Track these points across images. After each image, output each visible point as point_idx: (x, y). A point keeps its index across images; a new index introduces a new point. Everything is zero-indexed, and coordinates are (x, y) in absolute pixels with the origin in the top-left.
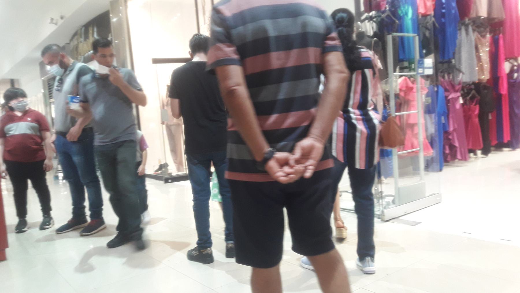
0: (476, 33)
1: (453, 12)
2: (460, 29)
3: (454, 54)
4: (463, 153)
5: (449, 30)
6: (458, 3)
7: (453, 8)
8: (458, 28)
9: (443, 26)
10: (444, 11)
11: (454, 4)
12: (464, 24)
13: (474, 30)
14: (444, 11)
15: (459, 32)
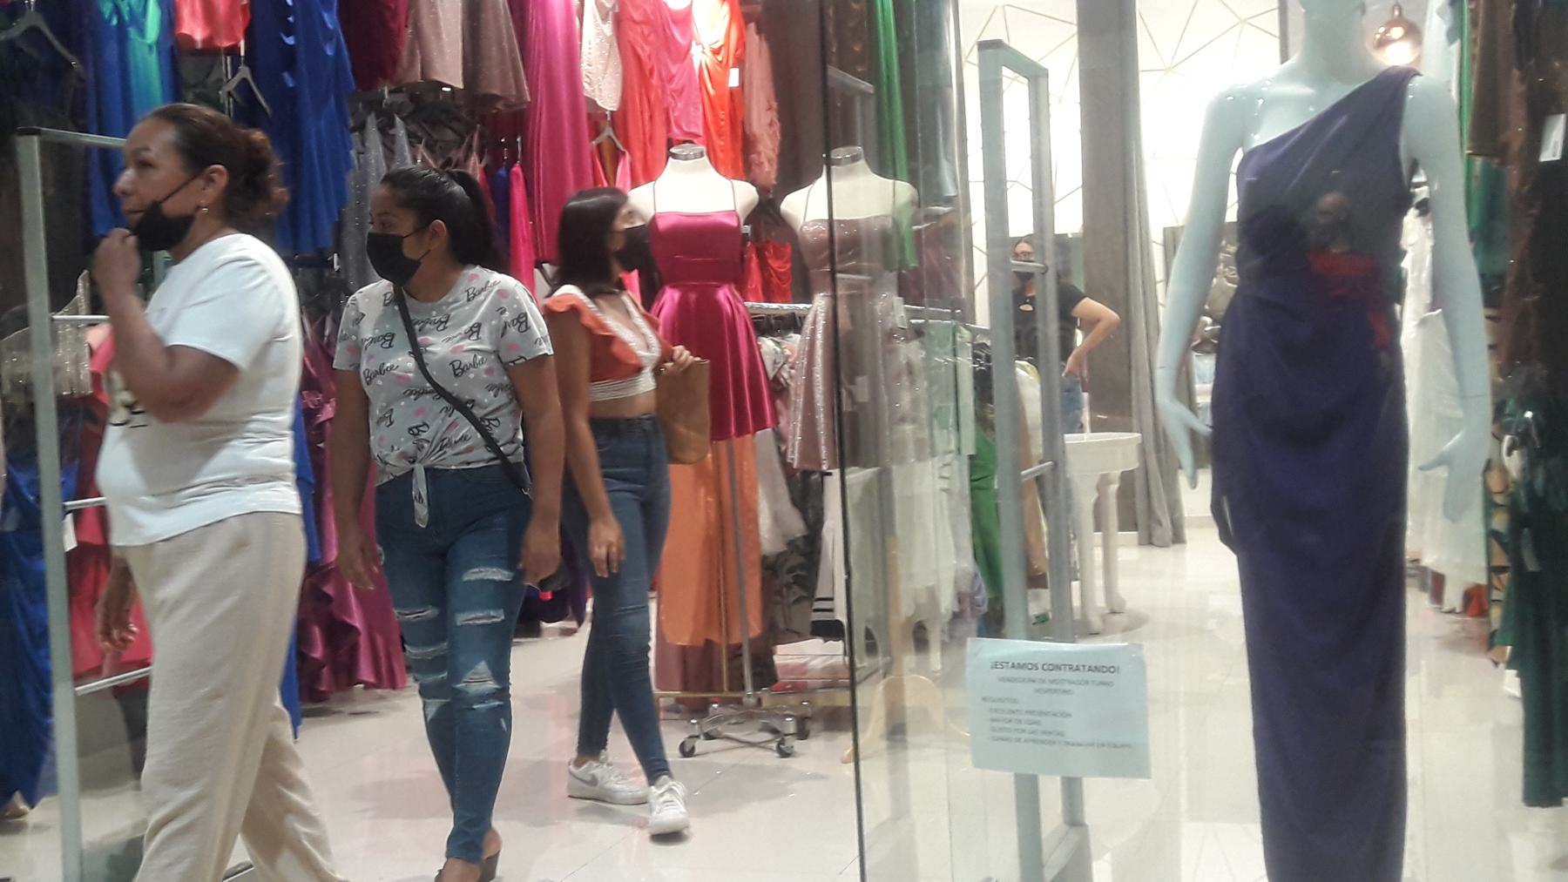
0: (421, 147)
1: (329, 52)
2: (361, 127)
3: (339, 227)
4: (382, 654)
5: (316, 127)
6: (345, 16)
7: (329, 36)
8: (351, 123)
9: (287, 102)
10: (290, 41)
11: (331, 20)
12: (375, 105)
13: (413, 138)
14: (290, 41)
15: (355, 136)
